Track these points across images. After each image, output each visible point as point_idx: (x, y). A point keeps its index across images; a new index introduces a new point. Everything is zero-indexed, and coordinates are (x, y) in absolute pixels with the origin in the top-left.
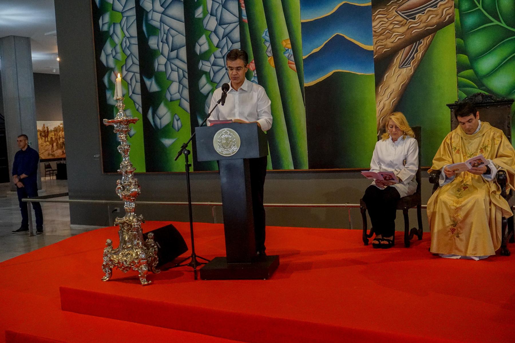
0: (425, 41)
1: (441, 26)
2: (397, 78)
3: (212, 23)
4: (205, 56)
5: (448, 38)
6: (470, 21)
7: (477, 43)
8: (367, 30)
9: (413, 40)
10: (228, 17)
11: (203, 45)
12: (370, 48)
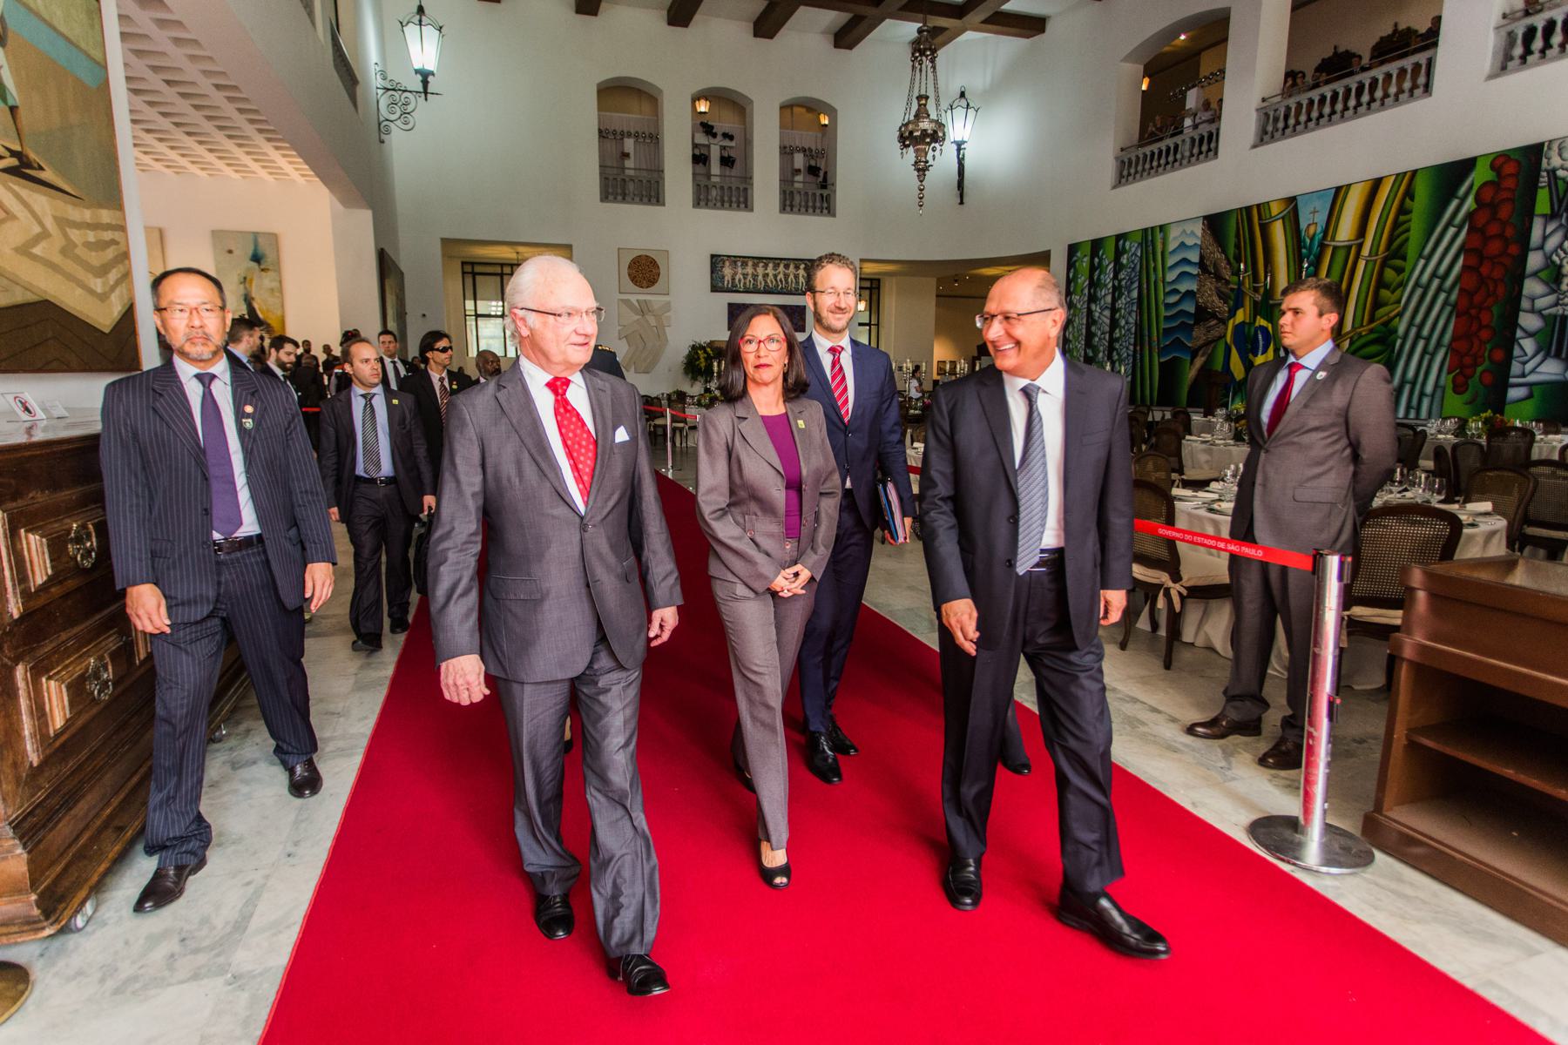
2: (1199, 361)
3: (1123, 322)
4: (1117, 340)
8: (1190, 337)
9: (1207, 344)
10: (1131, 320)
11: (1117, 334)
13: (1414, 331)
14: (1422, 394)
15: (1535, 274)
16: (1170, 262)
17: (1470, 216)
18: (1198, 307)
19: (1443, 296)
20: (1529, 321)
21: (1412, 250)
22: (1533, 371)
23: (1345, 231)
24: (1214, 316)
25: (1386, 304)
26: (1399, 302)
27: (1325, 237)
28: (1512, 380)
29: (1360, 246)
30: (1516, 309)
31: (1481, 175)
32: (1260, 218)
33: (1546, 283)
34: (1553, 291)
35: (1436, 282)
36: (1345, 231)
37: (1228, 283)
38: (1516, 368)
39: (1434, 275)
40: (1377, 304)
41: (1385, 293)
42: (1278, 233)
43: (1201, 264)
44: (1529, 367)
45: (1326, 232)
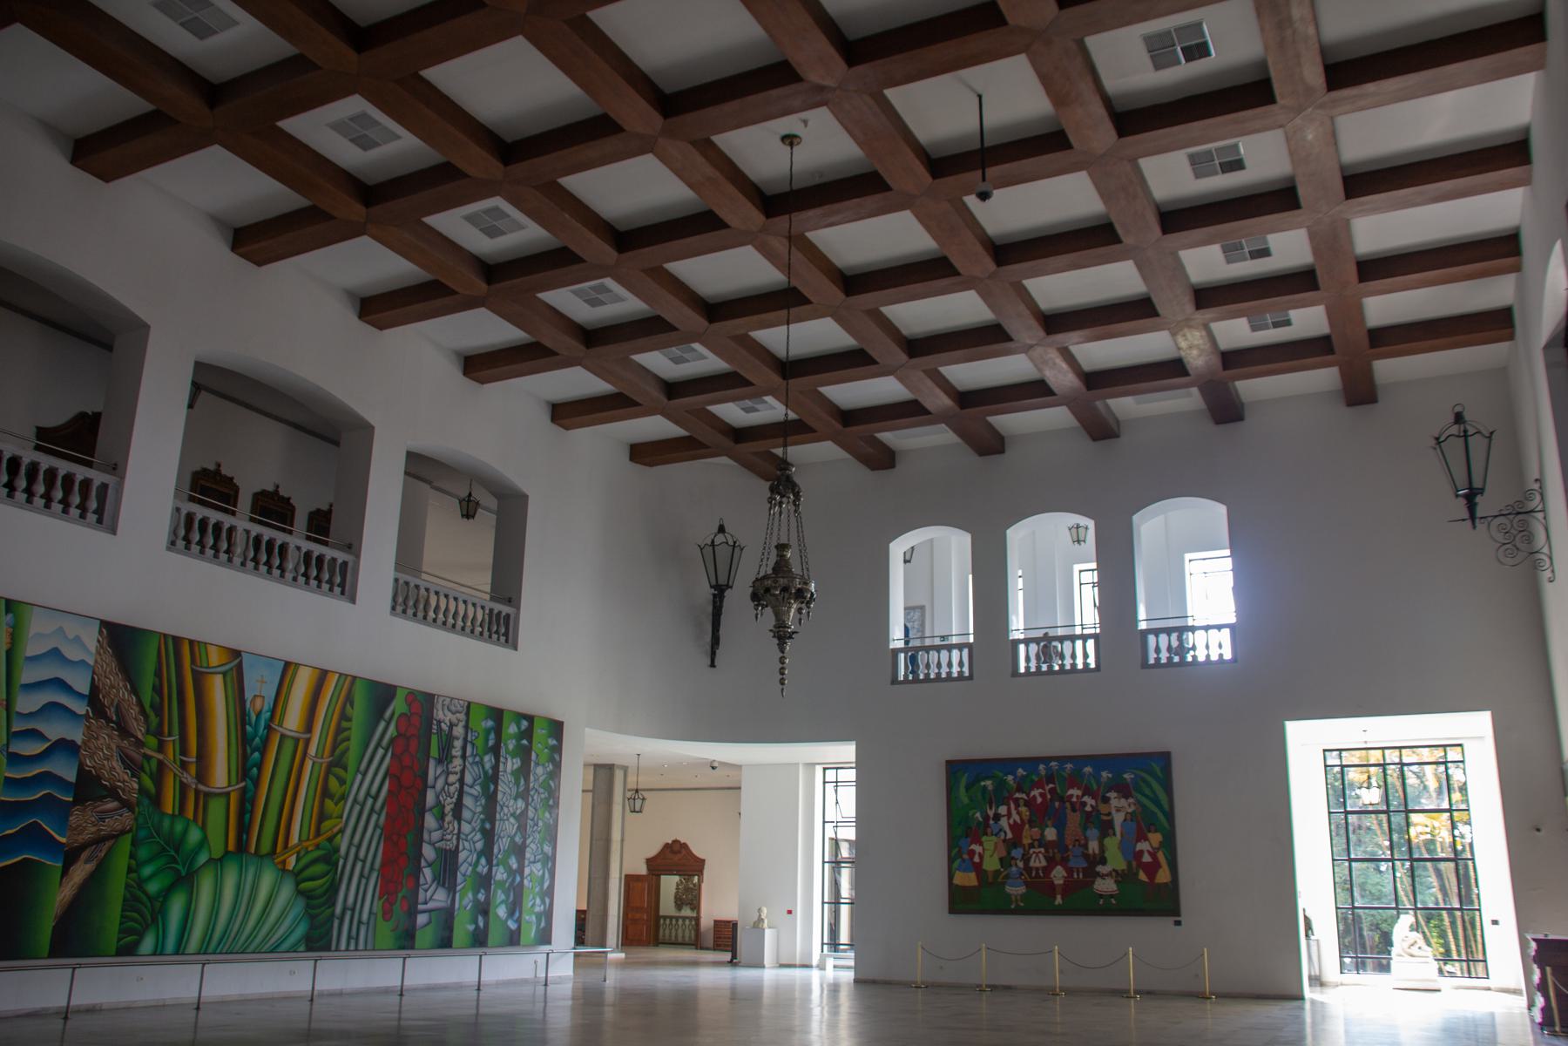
0: (108, 844)
1: (123, 832)
2: (80, 871)
5: (125, 844)
6: (143, 833)
7: (143, 853)
9: (98, 841)
12: (63, 840)
13: (353, 850)
14: (360, 922)
16: (27, 675)
17: (392, 740)
18: (82, 772)
19: (374, 817)
20: (428, 852)
23: (293, 720)
24: (113, 793)
25: (330, 817)
28: (421, 907)
29: (308, 742)
30: (422, 840)
31: (399, 706)
32: (193, 661)
34: (441, 827)
35: (370, 801)
36: (293, 720)
37: (140, 744)
39: (368, 794)
40: (322, 817)
41: (329, 803)
43: (94, 698)
45: (273, 711)
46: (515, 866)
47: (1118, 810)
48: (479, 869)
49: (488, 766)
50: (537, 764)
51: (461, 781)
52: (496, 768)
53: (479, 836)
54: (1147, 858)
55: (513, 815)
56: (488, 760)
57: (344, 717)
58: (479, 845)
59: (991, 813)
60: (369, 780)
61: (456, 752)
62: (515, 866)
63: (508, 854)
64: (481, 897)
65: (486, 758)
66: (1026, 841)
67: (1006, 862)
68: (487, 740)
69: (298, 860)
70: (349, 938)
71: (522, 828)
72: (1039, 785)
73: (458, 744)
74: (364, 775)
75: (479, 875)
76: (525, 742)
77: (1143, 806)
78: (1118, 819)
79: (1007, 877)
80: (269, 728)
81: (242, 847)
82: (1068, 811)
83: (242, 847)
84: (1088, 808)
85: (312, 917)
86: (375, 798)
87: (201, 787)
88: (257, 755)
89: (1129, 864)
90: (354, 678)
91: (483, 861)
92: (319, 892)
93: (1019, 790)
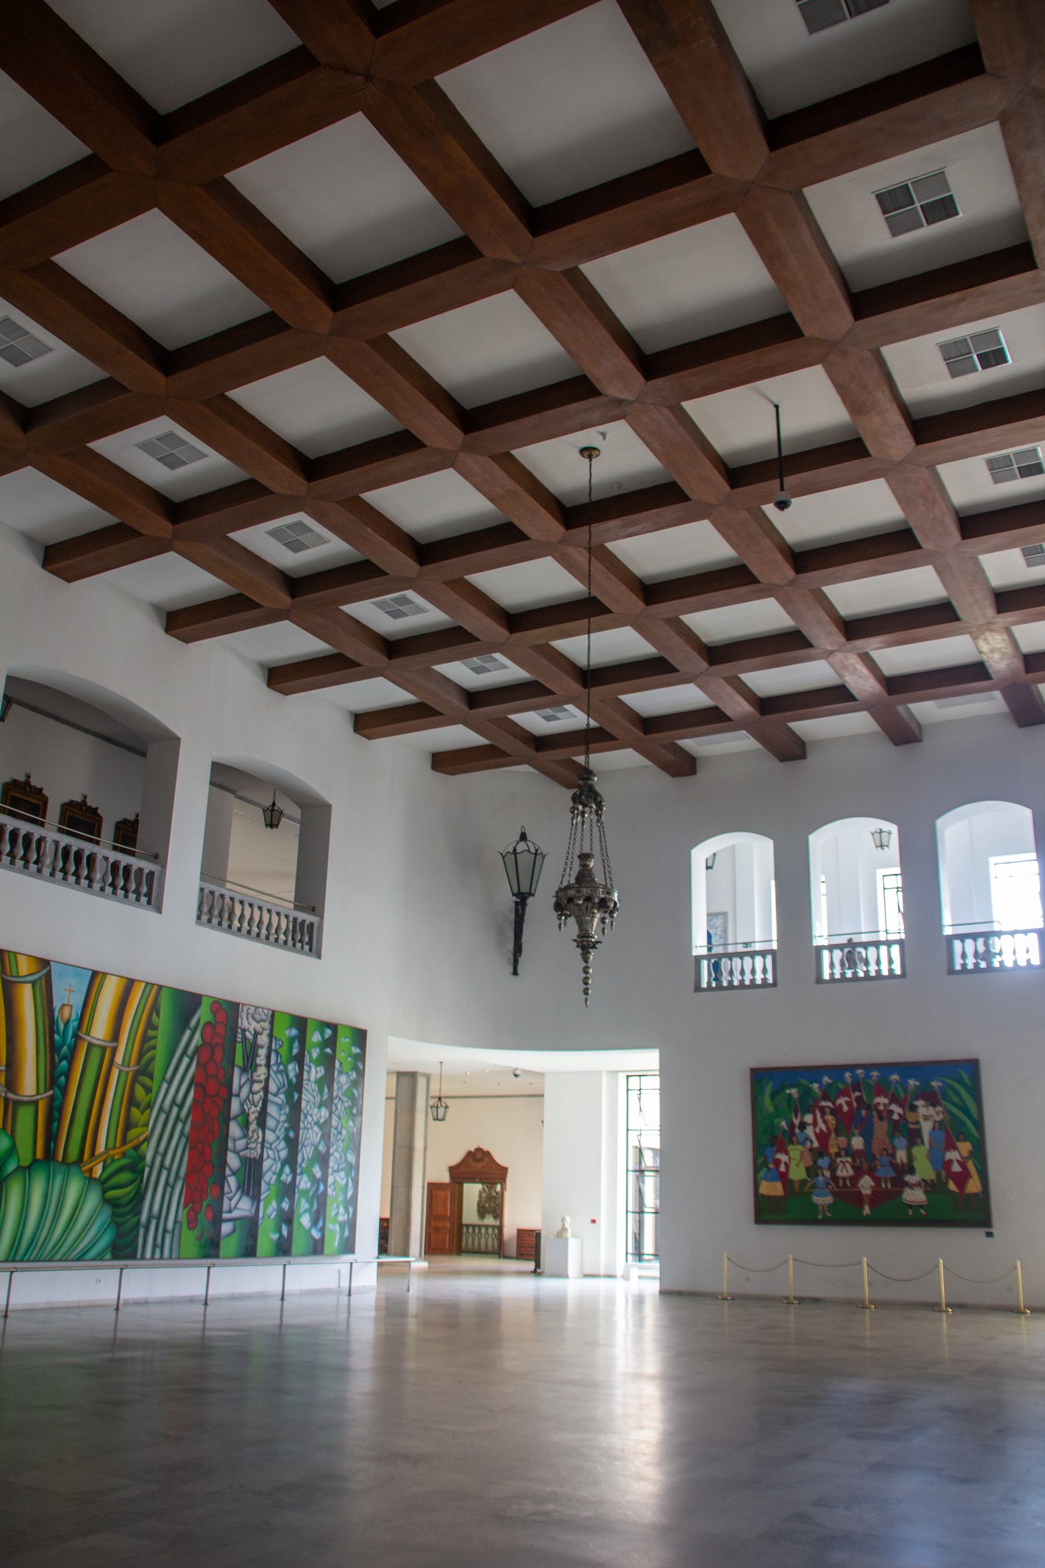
13: (159, 1159)
14: (165, 1231)
15: (235, 1118)
17: (198, 1049)
19: (180, 1126)
20: (233, 1161)
21: (157, 1067)
22: (235, 1207)
25: (136, 1126)
26: (147, 1125)
27: (80, 1027)
28: (225, 1216)
29: (114, 1050)
30: (226, 1149)
31: (204, 1014)
33: (242, 1128)
35: (175, 1110)
36: (100, 1029)
38: (226, 1206)
39: (173, 1102)
40: (128, 1125)
41: (135, 1112)
42: (27, 999)
44: (233, 1202)
45: (81, 1020)
46: (318, 1175)
47: (926, 1118)
48: (283, 1177)
49: (292, 1074)
50: (341, 1073)
51: (266, 1089)
52: (300, 1076)
53: (283, 1144)
54: (956, 1168)
55: (317, 1123)
56: (292, 1069)
57: (150, 1025)
58: (283, 1154)
59: (796, 1122)
60: (175, 1088)
61: (261, 1060)
62: (318, 1175)
63: (311, 1162)
64: (285, 1205)
65: (291, 1067)
66: (833, 1150)
67: (812, 1171)
68: (291, 1049)
69: (104, 1168)
70: (154, 1246)
71: (326, 1137)
72: (845, 1093)
73: (262, 1052)
74: (170, 1083)
75: (283, 1183)
76: (328, 1050)
77: (951, 1114)
78: (926, 1127)
79: (814, 1186)
80: (76, 1036)
81: (49, 1155)
82: (876, 1119)
83: (49, 1155)
84: (895, 1117)
85: (118, 1226)
86: (181, 1107)
87: (11, 1095)
88: (64, 1063)
89: (938, 1174)
90: (160, 987)
91: (287, 1169)
92: (125, 1200)
93: (825, 1097)
